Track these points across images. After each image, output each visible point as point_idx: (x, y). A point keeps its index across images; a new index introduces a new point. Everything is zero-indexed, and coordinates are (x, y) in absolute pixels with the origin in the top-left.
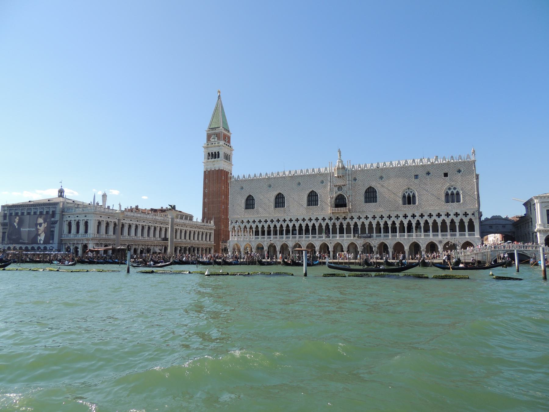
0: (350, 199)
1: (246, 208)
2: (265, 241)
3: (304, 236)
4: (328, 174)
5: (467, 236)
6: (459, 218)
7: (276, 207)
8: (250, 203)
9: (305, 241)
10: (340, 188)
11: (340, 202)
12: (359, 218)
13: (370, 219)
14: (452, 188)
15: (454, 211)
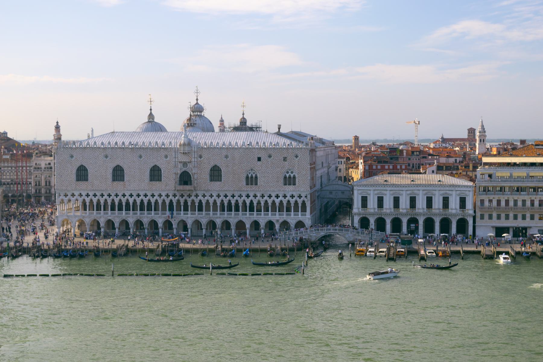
0: (196, 177)
1: (78, 180)
2: (103, 217)
3: (146, 212)
4: (173, 149)
5: (300, 216)
6: (294, 199)
7: (114, 180)
8: (82, 174)
9: (146, 218)
10: (185, 164)
11: (185, 179)
12: (204, 196)
13: (215, 197)
14: (290, 172)
15: (290, 193)
